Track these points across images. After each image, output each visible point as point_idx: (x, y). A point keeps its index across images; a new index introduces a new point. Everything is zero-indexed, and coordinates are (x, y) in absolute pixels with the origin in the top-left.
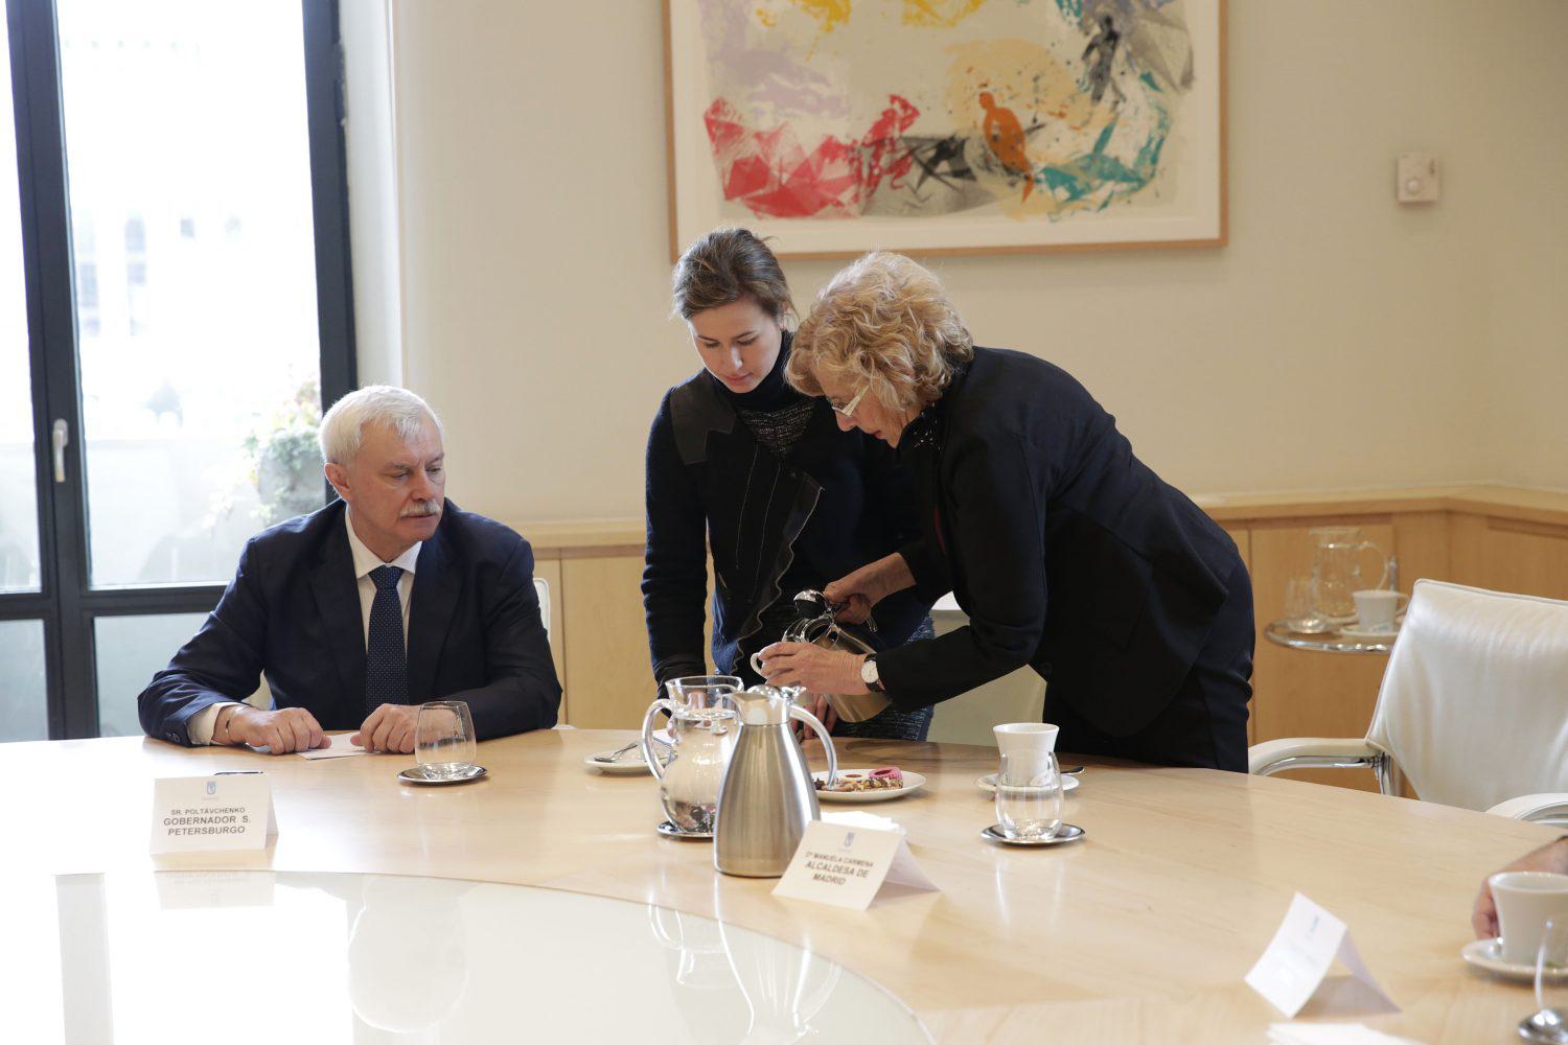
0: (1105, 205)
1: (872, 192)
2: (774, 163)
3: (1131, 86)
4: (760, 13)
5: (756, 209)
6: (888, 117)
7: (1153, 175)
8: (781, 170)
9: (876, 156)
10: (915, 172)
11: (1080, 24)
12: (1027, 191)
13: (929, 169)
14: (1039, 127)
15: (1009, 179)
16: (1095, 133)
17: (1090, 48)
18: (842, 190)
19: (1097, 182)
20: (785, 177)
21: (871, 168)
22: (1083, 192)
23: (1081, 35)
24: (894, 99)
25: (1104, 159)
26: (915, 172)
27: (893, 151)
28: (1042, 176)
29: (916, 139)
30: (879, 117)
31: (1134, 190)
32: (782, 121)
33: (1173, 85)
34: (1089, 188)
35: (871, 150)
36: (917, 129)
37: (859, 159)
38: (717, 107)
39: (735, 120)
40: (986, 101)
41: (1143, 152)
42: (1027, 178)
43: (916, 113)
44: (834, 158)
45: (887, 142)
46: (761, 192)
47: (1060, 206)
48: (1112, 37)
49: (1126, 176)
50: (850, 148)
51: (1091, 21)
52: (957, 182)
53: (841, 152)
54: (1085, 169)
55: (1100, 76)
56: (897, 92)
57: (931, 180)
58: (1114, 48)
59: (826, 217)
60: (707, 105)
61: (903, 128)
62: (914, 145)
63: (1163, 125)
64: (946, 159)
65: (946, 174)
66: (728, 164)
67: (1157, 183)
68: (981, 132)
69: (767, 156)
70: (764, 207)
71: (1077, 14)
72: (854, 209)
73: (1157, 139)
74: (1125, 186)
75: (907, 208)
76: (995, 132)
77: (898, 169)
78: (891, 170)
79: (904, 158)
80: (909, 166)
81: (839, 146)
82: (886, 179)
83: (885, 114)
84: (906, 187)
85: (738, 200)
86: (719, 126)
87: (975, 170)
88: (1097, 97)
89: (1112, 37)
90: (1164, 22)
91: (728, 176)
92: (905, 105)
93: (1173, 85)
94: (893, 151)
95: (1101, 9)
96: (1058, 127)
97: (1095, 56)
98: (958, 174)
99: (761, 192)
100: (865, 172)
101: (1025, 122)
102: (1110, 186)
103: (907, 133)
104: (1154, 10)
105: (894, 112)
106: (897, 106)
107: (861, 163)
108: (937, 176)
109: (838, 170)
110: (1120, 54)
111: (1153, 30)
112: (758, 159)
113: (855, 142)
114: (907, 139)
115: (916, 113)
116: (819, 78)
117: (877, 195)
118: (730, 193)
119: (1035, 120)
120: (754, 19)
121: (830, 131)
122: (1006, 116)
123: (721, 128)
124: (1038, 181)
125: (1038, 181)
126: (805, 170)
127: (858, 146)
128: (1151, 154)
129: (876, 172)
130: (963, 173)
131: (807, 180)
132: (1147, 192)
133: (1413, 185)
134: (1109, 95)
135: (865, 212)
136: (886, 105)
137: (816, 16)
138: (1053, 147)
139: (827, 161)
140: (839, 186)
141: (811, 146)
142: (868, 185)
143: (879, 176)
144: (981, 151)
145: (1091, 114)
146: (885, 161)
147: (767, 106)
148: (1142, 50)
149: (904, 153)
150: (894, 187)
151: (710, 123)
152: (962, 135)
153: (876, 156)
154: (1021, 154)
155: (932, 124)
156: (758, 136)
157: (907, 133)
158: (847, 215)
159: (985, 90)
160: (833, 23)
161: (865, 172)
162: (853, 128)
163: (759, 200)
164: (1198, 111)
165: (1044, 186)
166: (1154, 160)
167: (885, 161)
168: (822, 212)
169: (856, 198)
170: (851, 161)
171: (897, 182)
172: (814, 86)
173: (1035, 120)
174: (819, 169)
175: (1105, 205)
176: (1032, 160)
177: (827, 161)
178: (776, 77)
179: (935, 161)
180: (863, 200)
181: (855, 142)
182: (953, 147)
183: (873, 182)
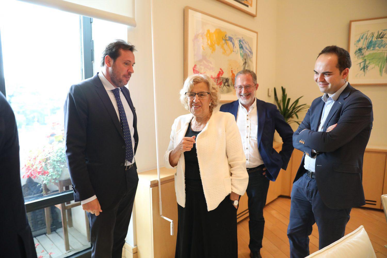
10: (223, 85)
26: (223, 85)
27: (220, 80)
45: (219, 78)
56: (221, 68)
57: (225, 86)
79: (221, 81)
92: (222, 71)
106: (221, 71)
113: (215, 77)
116: (211, 63)
130: (228, 86)
155: (225, 75)
171: (220, 86)
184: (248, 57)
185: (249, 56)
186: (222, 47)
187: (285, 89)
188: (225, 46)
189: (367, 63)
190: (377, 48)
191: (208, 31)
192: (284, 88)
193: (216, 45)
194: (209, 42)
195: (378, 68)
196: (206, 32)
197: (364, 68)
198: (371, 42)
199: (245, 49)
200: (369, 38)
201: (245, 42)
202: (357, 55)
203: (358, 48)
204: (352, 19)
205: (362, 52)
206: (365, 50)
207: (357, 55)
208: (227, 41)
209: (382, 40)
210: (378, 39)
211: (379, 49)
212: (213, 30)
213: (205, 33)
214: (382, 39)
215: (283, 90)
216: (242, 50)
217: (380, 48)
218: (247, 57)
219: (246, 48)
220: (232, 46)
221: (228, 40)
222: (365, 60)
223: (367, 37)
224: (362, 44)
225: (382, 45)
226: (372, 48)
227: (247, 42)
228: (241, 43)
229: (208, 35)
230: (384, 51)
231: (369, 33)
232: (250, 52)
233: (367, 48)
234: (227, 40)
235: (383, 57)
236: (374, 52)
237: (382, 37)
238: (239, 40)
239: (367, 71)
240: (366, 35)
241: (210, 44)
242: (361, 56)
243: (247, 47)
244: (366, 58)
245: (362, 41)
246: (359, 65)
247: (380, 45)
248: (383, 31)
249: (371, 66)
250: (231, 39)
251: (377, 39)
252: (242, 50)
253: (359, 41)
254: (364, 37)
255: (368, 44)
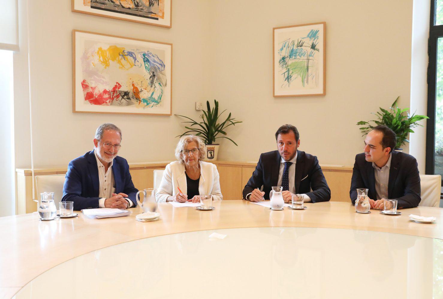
0: (152, 106)
1: (112, 101)
2: (94, 93)
3: (157, 85)
4: (93, 63)
5: (91, 103)
6: (116, 86)
7: (160, 102)
8: (96, 95)
9: (114, 94)
10: (120, 98)
11: (149, 73)
12: (140, 103)
13: (123, 97)
14: (142, 91)
15: (136, 100)
16: (151, 93)
17: (151, 77)
18: (107, 100)
19: (151, 102)
20: (97, 96)
21: (113, 96)
22: (149, 104)
23: (149, 75)
24: (117, 83)
25: (152, 98)
26: (120, 98)
27: (117, 93)
28: (142, 100)
29: (121, 91)
30: (114, 86)
31: (157, 104)
32: (96, 85)
33: (163, 85)
34: (150, 103)
35: (112, 93)
36: (121, 89)
37: (110, 94)
38: (84, 81)
39: (87, 84)
40: (133, 85)
41: (159, 97)
42: (140, 100)
43: (121, 86)
44: (106, 94)
45: (116, 91)
46: (92, 99)
47: (145, 106)
48: (154, 76)
49: (156, 102)
50: (109, 92)
51: (151, 72)
52: (128, 100)
53: (107, 92)
54: (149, 99)
55: (152, 82)
56: (118, 82)
57: (123, 99)
58: (154, 78)
59: (104, 105)
60: (82, 81)
61: (118, 89)
62: (121, 92)
63: (162, 93)
64: (126, 95)
65: (126, 98)
66: (86, 93)
67: (161, 103)
68: (132, 91)
69: (93, 92)
70: (92, 102)
71: (149, 71)
72: (109, 104)
73: (161, 95)
74: (156, 103)
75: (119, 105)
76: (135, 91)
77: (117, 97)
78: (116, 97)
79: (118, 95)
80: (119, 96)
81: (107, 91)
82: (115, 98)
83: (115, 86)
84: (119, 101)
85: (87, 100)
86: (84, 85)
87: (131, 98)
88: (152, 86)
89: (154, 76)
90: (162, 74)
91: (85, 96)
92: (119, 84)
93: (163, 85)
94: (117, 93)
95: (152, 70)
96: (145, 91)
97: (151, 79)
98: (128, 99)
99: (92, 99)
100: (111, 97)
101: (140, 90)
102: (153, 103)
103: (119, 90)
104: (161, 72)
105: (117, 85)
106: (118, 84)
107: (111, 95)
108: (124, 99)
109: (106, 96)
110: (155, 79)
111: (161, 75)
112: (91, 92)
113: (110, 91)
114: (119, 91)
115: (121, 86)
116: (103, 77)
117: (113, 101)
118: (86, 99)
119: (141, 90)
120: (92, 65)
121: (105, 88)
122: (136, 88)
123: (85, 85)
124: (142, 101)
125: (142, 101)
126: (100, 95)
127: (110, 91)
128: (160, 98)
129: (113, 97)
130: (129, 98)
131: (101, 97)
132: (159, 105)
133: (199, 107)
134: (153, 86)
135: (111, 105)
136: (116, 84)
137: (103, 65)
138: (144, 95)
139: (105, 94)
140: (107, 99)
141: (102, 91)
142: (112, 99)
143: (114, 98)
144: (132, 95)
145: (150, 89)
146: (115, 95)
147: (94, 82)
148: (159, 79)
149: (118, 94)
150: (117, 100)
151: (83, 84)
152: (129, 91)
153: (114, 94)
154: (139, 96)
155: (124, 89)
156: (92, 88)
157: (119, 90)
158: (108, 105)
159: (133, 83)
160: (107, 67)
161: (111, 97)
162: (110, 88)
163: (92, 101)
164: (167, 90)
165: (142, 102)
166: (160, 99)
167: (115, 95)
168: (103, 104)
169: (110, 102)
170: (109, 94)
172: (102, 79)
173: (141, 90)
174: (103, 96)
175: (152, 106)
176: (141, 97)
177: (105, 94)
178: (95, 76)
179: (124, 96)
180: (111, 102)
181: (110, 91)
182: (127, 93)
183: (113, 99)
184: (158, 70)
185: (159, 68)
186: (119, 62)
187: (218, 102)
188: (123, 61)
189: (290, 72)
190: (298, 57)
191: (100, 49)
192: (217, 101)
193: (111, 62)
194: (101, 59)
195: (300, 78)
196: (97, 50)
197: (288, 78)
198: (292, 50)
199: (152, 62)
200: (291, 46)
201: (153, 56)
202: (281, 64)
203: (282, 57)
204: (274, 27)
205: (285, 61)
206: (288, 59)
207: (281, 64)
208: (125, 56)
209: (301, 48)
210: (298, 48)
211: (300, 58)
212: (105, 47)
213: (96, 51)
214: (302, 47)
215: (216, 103)
216: (148, 63)
217: (300, 57)
218: (156, 70)
219: (155, 61)
220: (133, 60)
221: (127, 55)
222: (289, 69)
223: (289, 46)
224: (285, 53)
225: (302, 54)
226: (294, 57)
227: (155, 55)
228: (146, 56)
229: (100, 52)
230: (304, 60)
231: (291, 41)
232: (161, 65)
233: (289, 57)
234: (126, 55)
235: (304, 66)
236: (294, 61)
237: (301, 46)
238: (142, 54)
239: (291, 81)
240: (288, 43)
241: (102, 60)
242: (285, 65)
243: (156, 60)
244: (289, 67)
245: (285, 49)
246: (284, 74)
247: (301, 54)
248: (302, 40)
249: (294, 76)
250: (130, 54)
251: (297, 47)
252: (147, 64)
253: (282, 49)
254: (286, 45)
255: (290, 52)
